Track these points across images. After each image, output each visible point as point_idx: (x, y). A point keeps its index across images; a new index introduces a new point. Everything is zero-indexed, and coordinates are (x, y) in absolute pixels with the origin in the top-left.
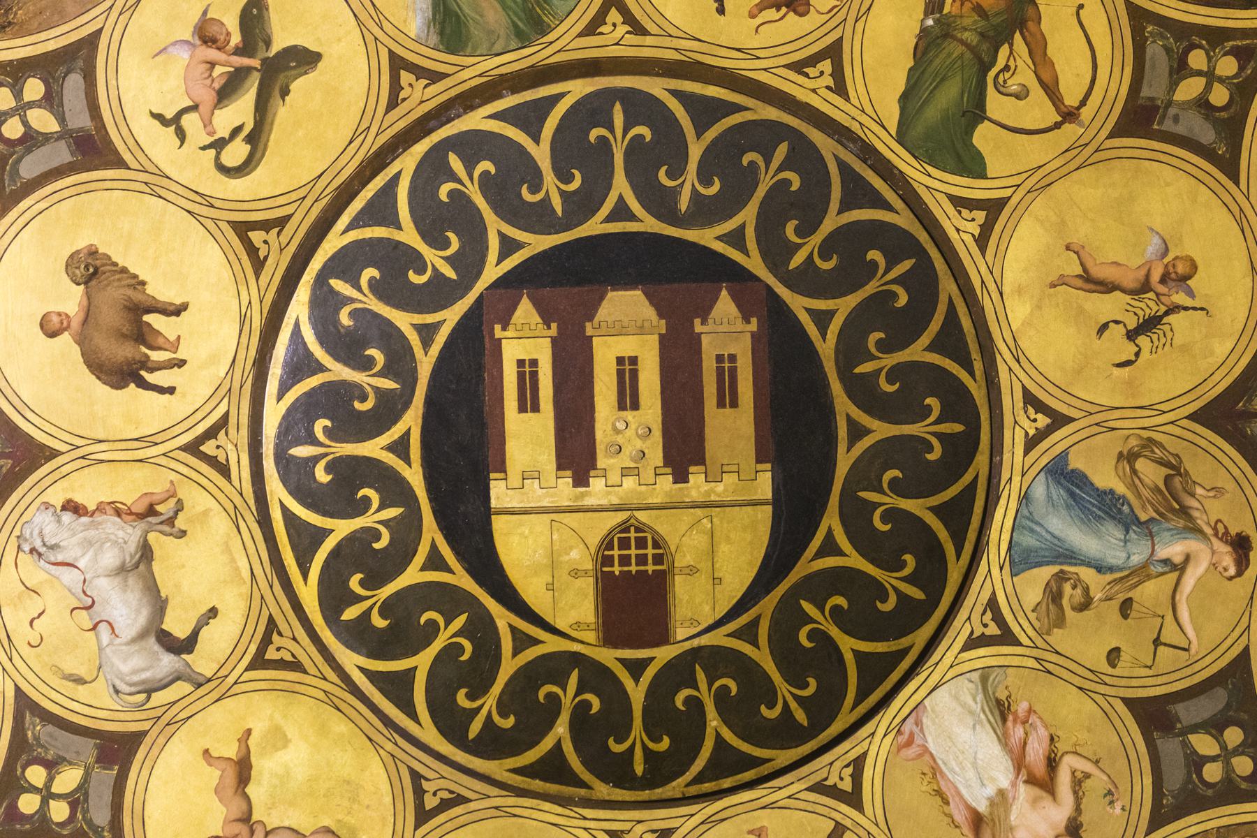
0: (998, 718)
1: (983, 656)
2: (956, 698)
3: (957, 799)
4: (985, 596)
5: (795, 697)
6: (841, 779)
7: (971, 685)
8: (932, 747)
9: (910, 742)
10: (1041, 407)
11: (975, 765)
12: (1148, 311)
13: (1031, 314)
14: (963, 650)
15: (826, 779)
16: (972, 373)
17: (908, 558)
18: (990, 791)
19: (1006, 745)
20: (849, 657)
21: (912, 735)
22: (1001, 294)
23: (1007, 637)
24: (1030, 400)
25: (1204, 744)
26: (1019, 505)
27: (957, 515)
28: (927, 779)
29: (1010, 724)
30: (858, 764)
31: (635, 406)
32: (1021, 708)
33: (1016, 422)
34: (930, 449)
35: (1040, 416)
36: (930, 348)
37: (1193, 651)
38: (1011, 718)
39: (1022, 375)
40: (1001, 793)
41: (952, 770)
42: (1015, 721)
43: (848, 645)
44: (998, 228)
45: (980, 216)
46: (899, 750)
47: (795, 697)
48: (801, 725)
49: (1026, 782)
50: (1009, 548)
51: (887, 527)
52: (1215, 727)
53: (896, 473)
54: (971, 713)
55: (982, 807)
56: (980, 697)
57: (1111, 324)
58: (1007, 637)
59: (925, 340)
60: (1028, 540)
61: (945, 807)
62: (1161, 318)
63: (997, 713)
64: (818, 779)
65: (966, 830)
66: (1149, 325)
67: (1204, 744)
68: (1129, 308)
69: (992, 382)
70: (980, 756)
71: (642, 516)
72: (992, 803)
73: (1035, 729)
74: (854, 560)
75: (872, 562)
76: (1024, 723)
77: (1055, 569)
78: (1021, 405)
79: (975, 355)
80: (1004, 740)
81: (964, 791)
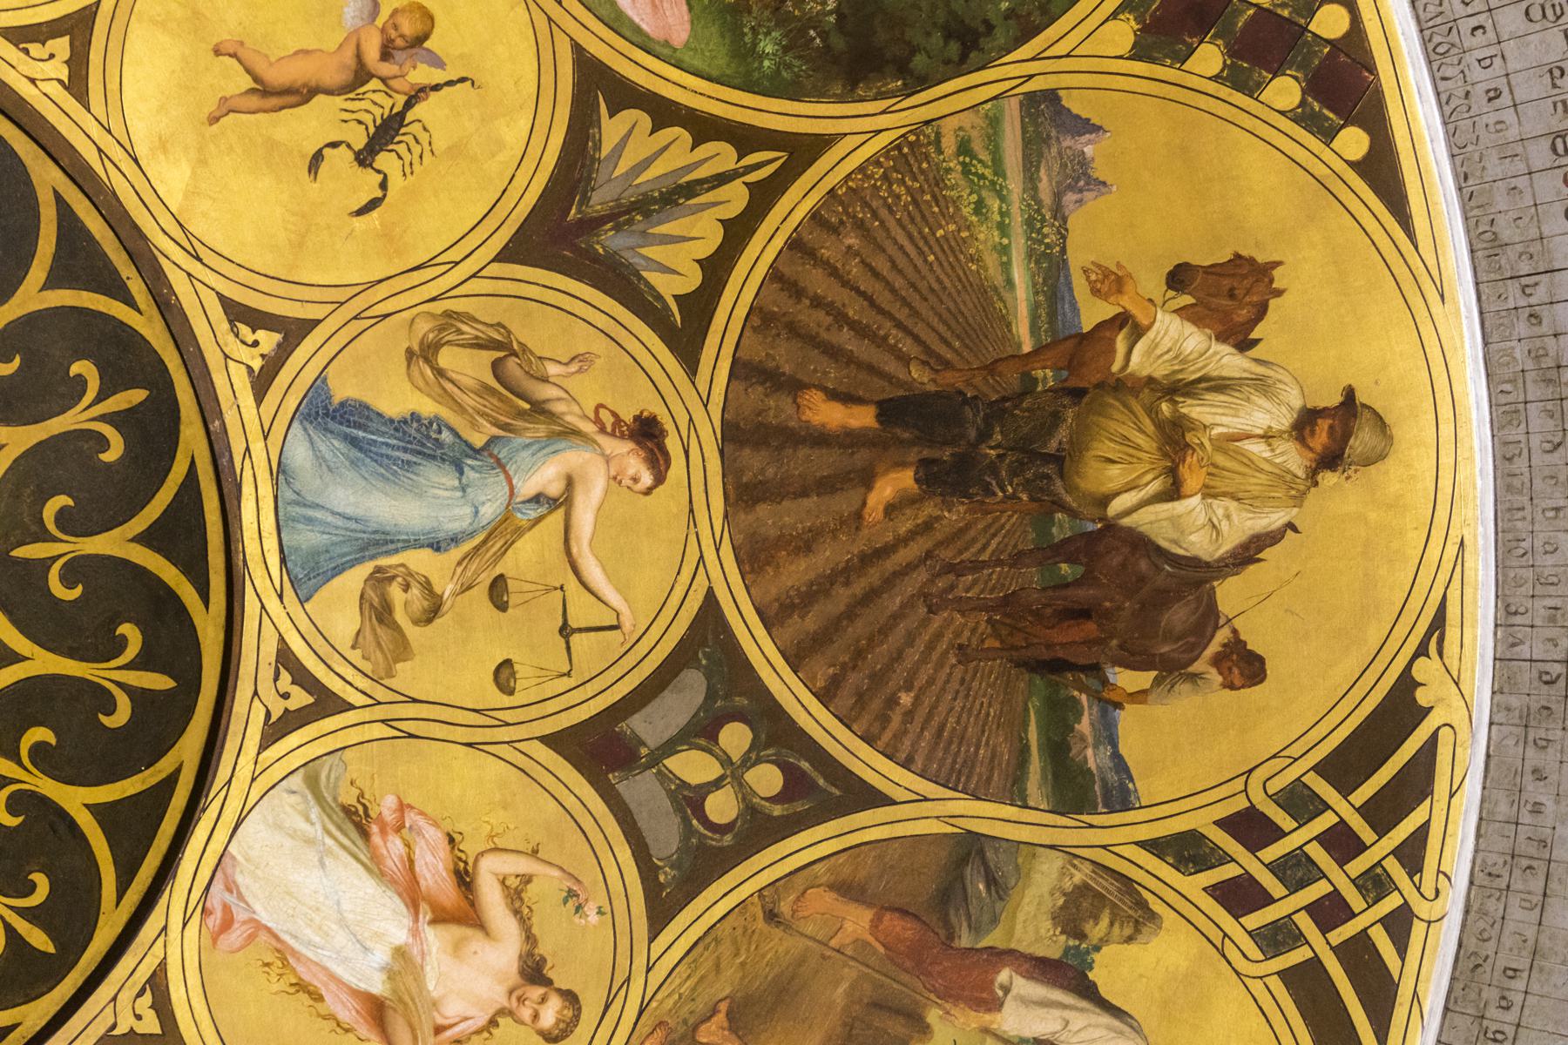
0: (354, 834)
1: (298, 745)
2: (278, 826)
3: (333, 986)
4: (270, 649)
5: (21, 912)
6: (139, 1017)
7: (294, 799)
8: (264, 917)
9: (227, 923)
10: (258, 319)
11: (342, 922)
12: (378, 112)
13: (194, 173)
14: (263, 747)
15: (114, 1026)
16: (130, 302)
17: (128, 630)
18: (381, 956)
19: (383, 874)
20: (86, 821)
21: (226, 908)
22: (136, 160)
23: (326, 703)
24: (237, 313)
25: (693, 766)
26: (276, 485)
27: (180, 534)
28: (274, 971)
29: (376, 839)
30: (157, 984)
32: (386, 807)
33: (226, 357)
34: (104, 444)
35: (261, 335)
36: (51, 283)
37: (627, 626)
38: (375, 829)
39: (211, 278)
40: (400, 953)
41: (309, 943)
42: (383, 832)
43: (75, 800)
44: (95, 57)
45: (61, 46)
46: (215, 941)
47: (21, 912)
48: (45, 954)
49: (433, 922)
50: (283, 561)
51: (77, 592)
52: (702, 732)
53: (62, 500)
54: (310, 842)
55: (377, 986)
56: (315, 813)
57: (326, 151)
58: (326, 703)
59: (38, 272)
60: (305, 539)
61: (319, 1005)
62: (401, 115)
63: (350, 827)
64: (102, 1031)
65: (364, 1030)
66: (387, 132)
67: (693, 766)
68: (346, 116)
69: (168, 303)
70: (346, 906)
72: (391, 975)
73: (420, 833)
74: (43, 662)
75: (72, 654)
76: (399, 828)
77: (366, 569)
78: (226, 326)
79: (126, 270)
80: (375, 867)
81: (339, 970)
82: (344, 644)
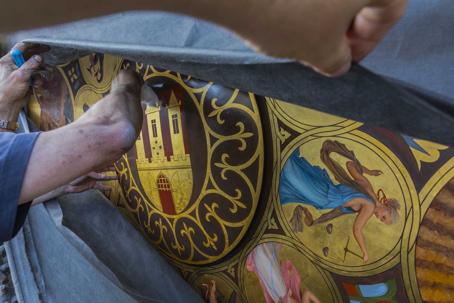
10: (287, 129)
23: (280, 231)
31: (157, 136)
58: (280, 231)
71: (164, 172)
82: (289, 219)
